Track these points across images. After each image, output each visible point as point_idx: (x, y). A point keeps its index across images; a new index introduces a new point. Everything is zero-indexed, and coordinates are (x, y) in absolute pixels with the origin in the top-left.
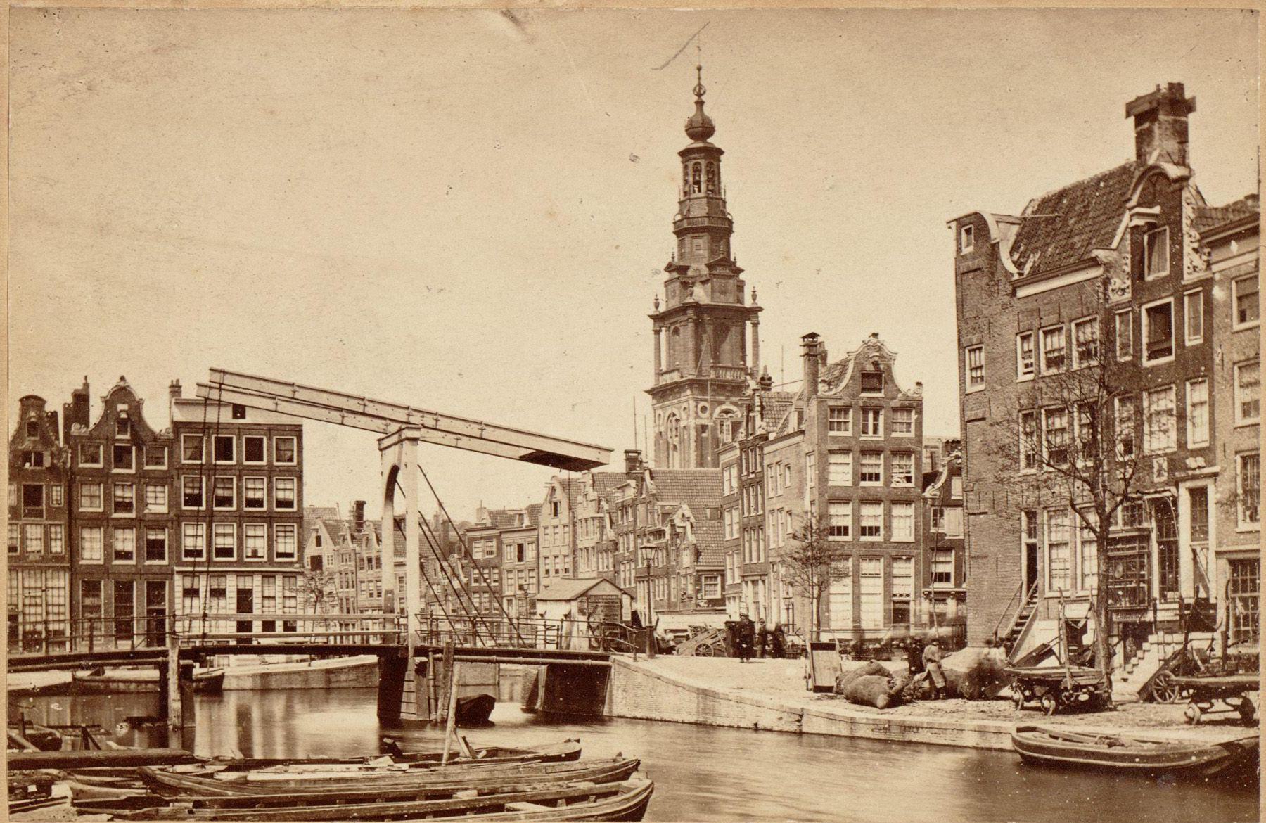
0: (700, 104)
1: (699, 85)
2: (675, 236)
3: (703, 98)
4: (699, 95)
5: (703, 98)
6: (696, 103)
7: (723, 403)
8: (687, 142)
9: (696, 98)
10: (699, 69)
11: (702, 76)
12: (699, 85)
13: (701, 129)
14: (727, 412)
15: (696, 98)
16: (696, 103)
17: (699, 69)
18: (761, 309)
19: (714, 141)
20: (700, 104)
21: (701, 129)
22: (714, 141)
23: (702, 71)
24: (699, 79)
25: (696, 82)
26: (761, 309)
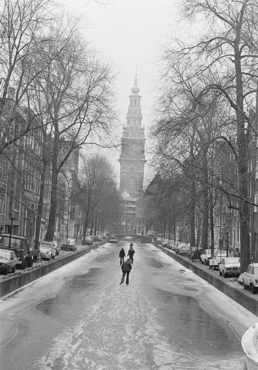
0: (136, 84)
1: (136, 78)
2: (126, 119)
4: (136, 80)
6: (135, 83)
8: (131, 94)
9: (135, 82)
10: (136, 74)
12: (136, 78)
13: (136, 91)
14: (132, 168)
17: (136, 74)
19: (139, 94)
20: (136, 84)
21: (136, 91)
22: (139, 94)
24: (136, 77)
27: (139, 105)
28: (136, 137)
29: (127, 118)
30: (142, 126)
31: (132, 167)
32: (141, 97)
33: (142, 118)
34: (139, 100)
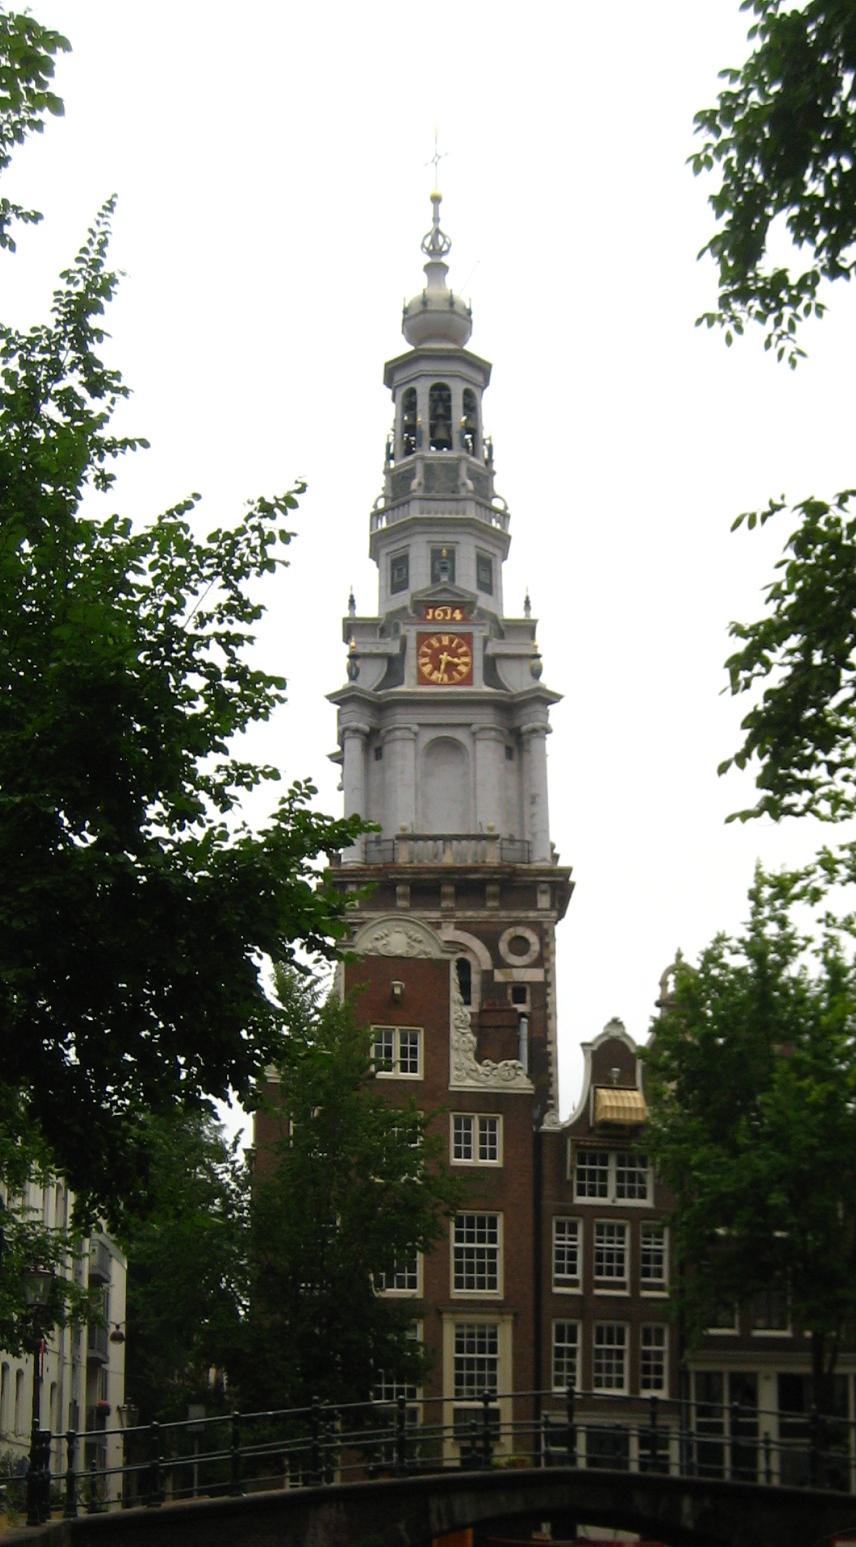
0: (436, 269)
1: (438, 232)
3: (444, 259)
5: (444, 259)
6: (428, 268)
9: (428, 259)
10: (436, 200)
11: (441, 215)
15: (428, 259)
16: (428, 268)
17: (436, 200)
18: (552, 698)
20: (436, 269)
23: (441, 206)
24: (436, 219)
25: (429, 227)
26: (552, 698)
30: (512, 610)
34: (468, 394)
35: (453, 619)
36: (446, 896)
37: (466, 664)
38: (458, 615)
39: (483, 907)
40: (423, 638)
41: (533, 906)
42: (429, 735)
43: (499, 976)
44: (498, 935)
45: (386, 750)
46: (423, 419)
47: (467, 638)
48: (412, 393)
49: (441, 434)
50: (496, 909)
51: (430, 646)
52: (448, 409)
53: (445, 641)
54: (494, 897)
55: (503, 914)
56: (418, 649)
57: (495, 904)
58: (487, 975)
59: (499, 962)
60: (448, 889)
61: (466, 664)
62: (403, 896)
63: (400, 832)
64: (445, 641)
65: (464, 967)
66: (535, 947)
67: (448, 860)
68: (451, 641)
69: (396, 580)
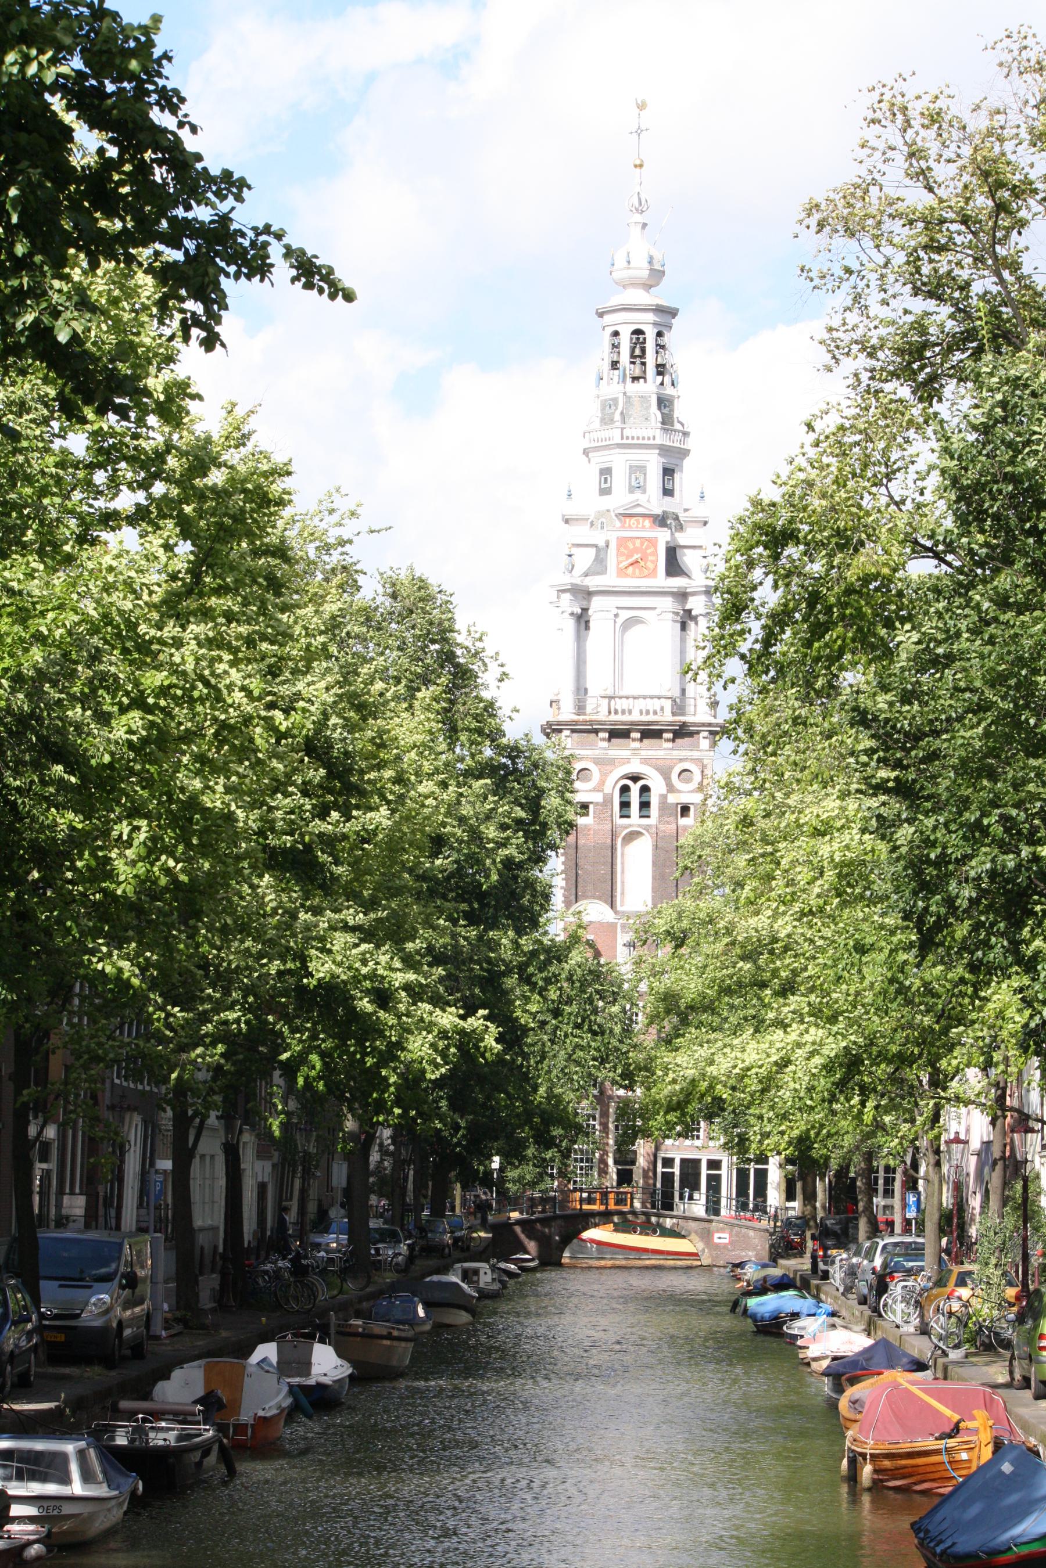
7: (628, 760)
14: (635, 779)
27: (661, 369)
28: (653, 574)
29: (586, 452)
31: (635, 767)
32: (673, 313)
33: (685, 453)
34: (660, 334)
35: (643, 527)
36: (634, 740)
37: (652, 562)
38: (647, 523)
39: (660, 749)
40: (622, 542)
41: (696, 747)
42: (625, 615)
43: (672, 799)
44: (671, 768)
45: (592, 624)
46: (625, 358)
47: (653, 542)
48: (616, 334)
49: (637, 373)
50: (672, 749)
51: (626, 548)
52: (643, 350)
53: (638, 543)
54: (668, 740)
55: (675, 753)
56: (618, 549)
57: (670, 745)
58: (663, 798)
59: (671, 788)
60: (638, 735)
61: (652, 562)
62: (603, 739)
63: (603, 693)
64: (638, 543)
65: (645, 789)
66: (697, 777)
67: (635, 717)
68: (642, 544)
69: (603, 486)
